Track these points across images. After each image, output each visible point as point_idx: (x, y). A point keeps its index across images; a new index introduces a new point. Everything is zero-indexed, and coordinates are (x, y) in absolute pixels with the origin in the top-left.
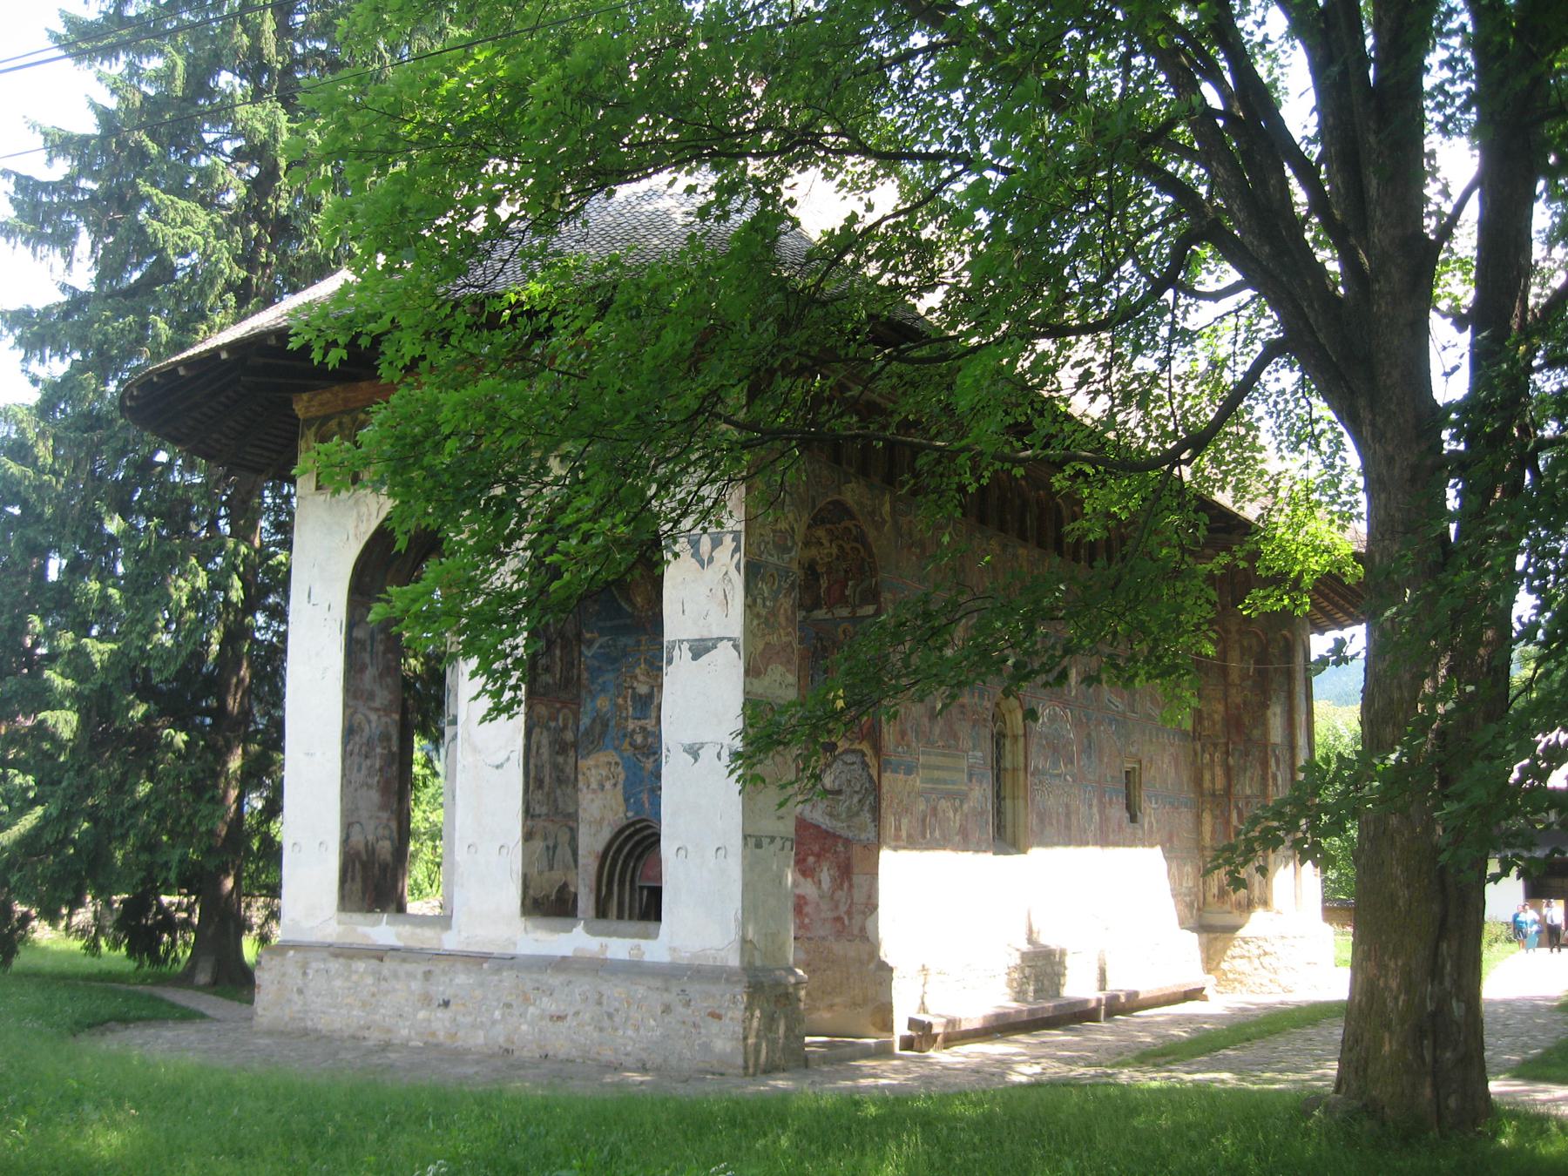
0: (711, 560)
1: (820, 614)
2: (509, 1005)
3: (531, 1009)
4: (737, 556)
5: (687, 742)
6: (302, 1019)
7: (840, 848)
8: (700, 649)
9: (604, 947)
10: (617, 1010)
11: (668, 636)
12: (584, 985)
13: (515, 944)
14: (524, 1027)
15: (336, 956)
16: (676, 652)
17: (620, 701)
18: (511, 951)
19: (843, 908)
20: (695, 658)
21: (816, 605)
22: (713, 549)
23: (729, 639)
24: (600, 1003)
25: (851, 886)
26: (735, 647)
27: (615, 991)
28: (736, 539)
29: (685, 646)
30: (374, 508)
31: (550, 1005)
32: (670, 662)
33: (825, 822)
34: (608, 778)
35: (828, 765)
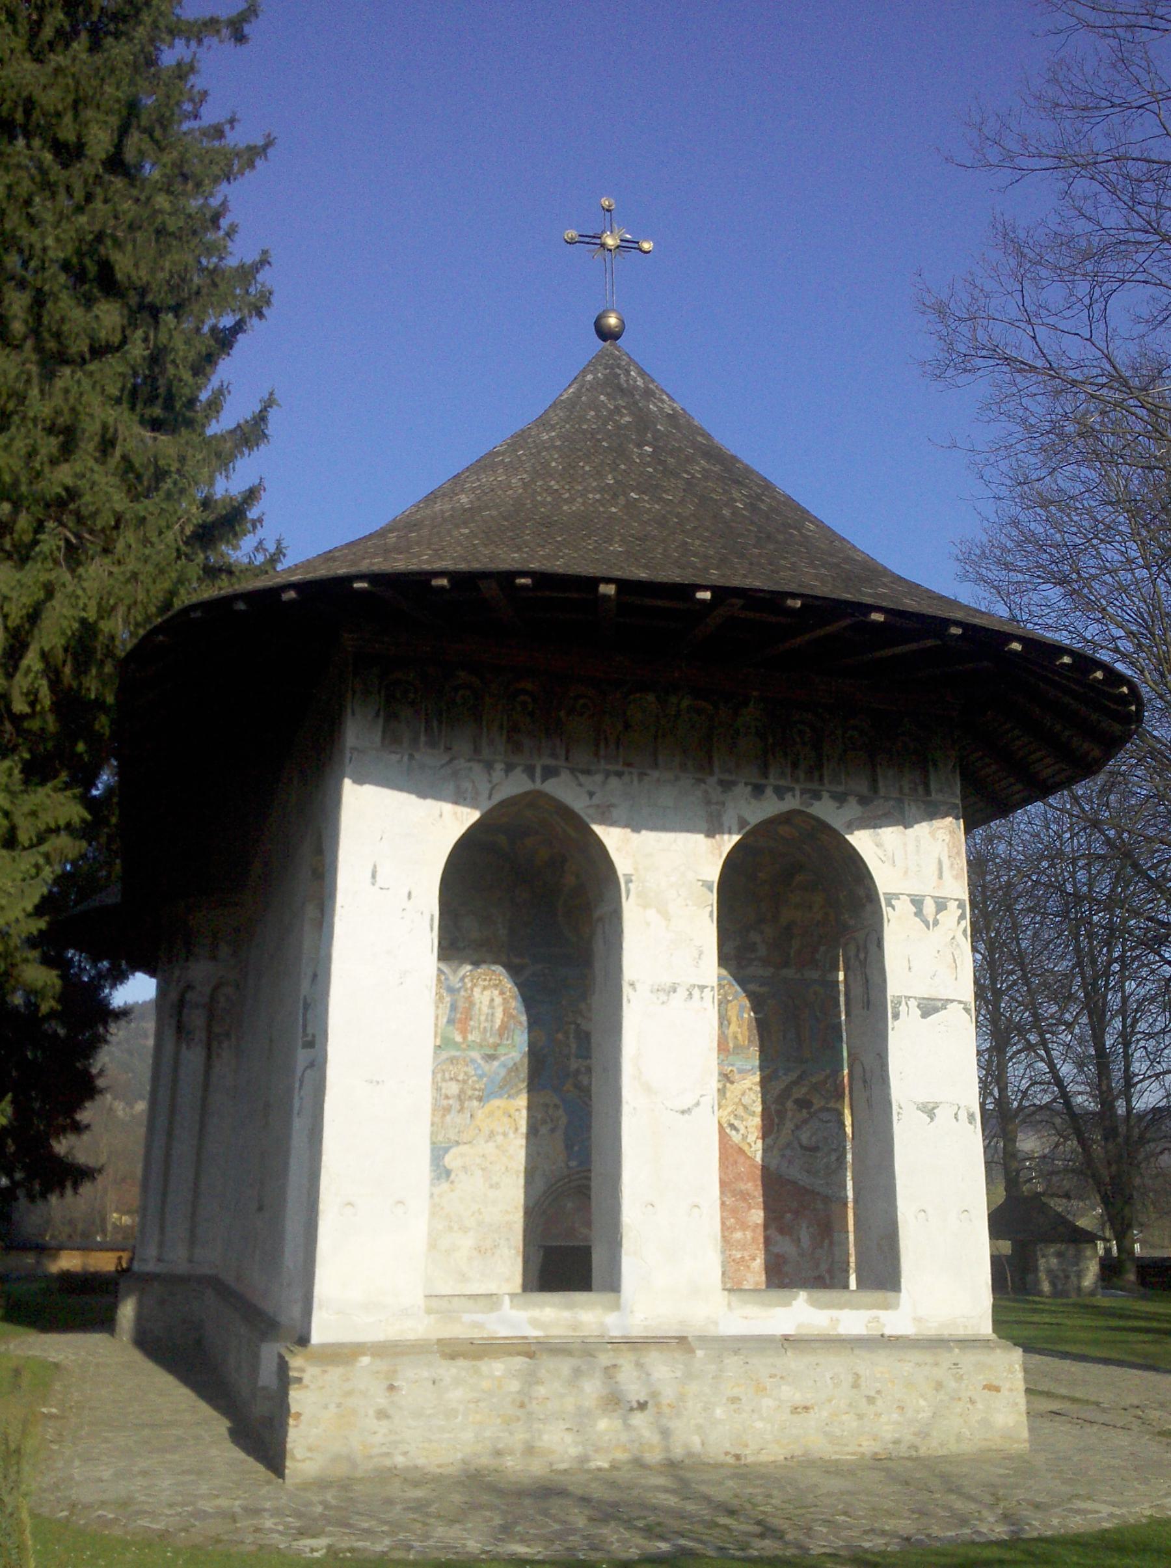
0: (936, 922)
1: (789, 973)
2: (735, 1400)
3: (767, 1403)
4: (963, 923)
5: (922, 1099)
6: (388, 1454)
7: (820, 1206)
8: (929, 1008)
9: (835, 1321)
10: (878, 1392)
11: (894, 988)
12: (835, 1365)
13: (716, 1324)
14: (759, 1425)
15: (453, 1357)
16: (903, 1008)
17: (560, 1036)
18: (713, 1331)
19: (824, 1267)
20: (925, 1015)
21: (786, 964)
22: (937, 913)
23: (960, 1002)
24: (856, 1386)
25: (831, 1243)
26: (967, 1010)
27: (879, 1369)
28: (961, 906)
29: (913, 1003)
30: (484, 788)
31: (790, 1394)
32: (896, 1016)
33: (804, 1179)
34: (544, 1122)
35: (805, 1122)
